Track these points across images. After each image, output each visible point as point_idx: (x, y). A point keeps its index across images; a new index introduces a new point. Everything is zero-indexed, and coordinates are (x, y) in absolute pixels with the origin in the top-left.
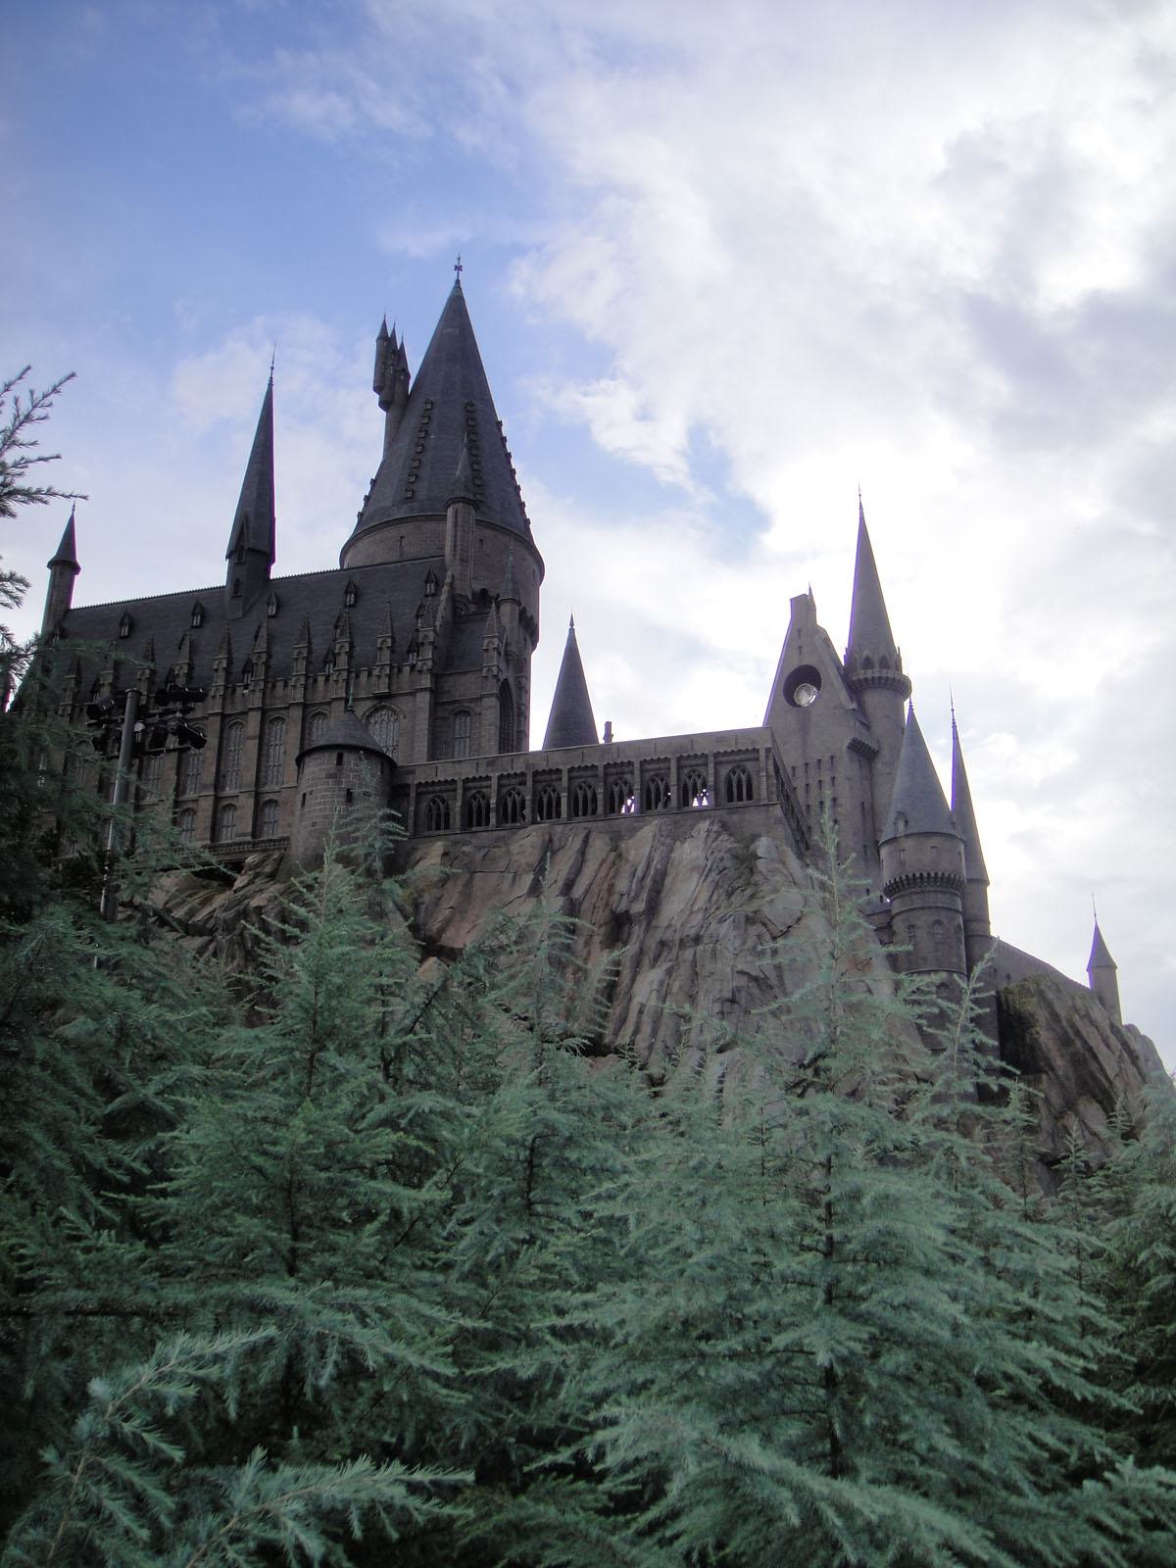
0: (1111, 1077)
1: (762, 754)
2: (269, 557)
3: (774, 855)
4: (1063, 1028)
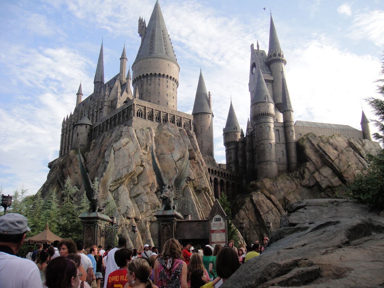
0: (333, 159)
1: (133, 105)
2: (102, 82)
3: (127, 130)
4: (315, 147)
